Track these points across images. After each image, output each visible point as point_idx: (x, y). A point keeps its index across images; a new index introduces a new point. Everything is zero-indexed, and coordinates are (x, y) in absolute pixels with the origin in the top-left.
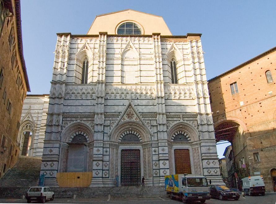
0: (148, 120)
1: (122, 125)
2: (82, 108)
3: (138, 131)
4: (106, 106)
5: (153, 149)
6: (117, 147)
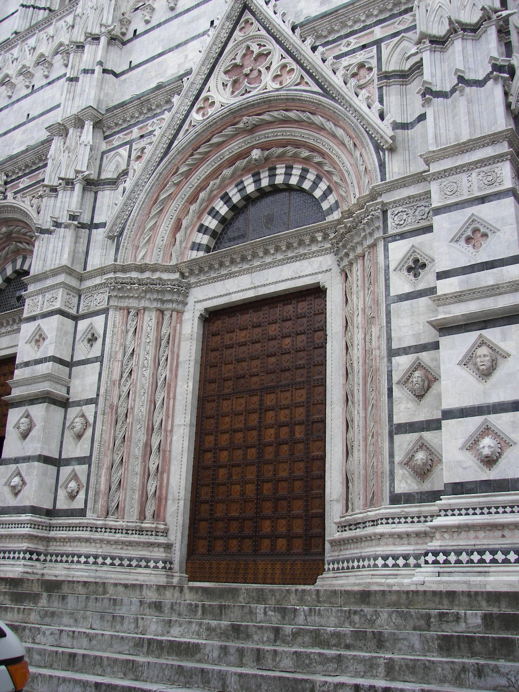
0: (364, 47)
1: (194, 146)
2: (24, 132)
3: (305, 153)
4: (123, 73)
5: (399, 250)
6: (169, 295)
